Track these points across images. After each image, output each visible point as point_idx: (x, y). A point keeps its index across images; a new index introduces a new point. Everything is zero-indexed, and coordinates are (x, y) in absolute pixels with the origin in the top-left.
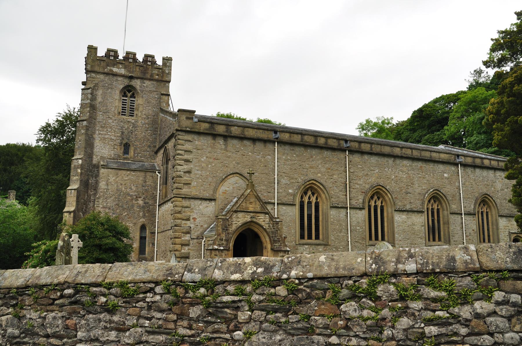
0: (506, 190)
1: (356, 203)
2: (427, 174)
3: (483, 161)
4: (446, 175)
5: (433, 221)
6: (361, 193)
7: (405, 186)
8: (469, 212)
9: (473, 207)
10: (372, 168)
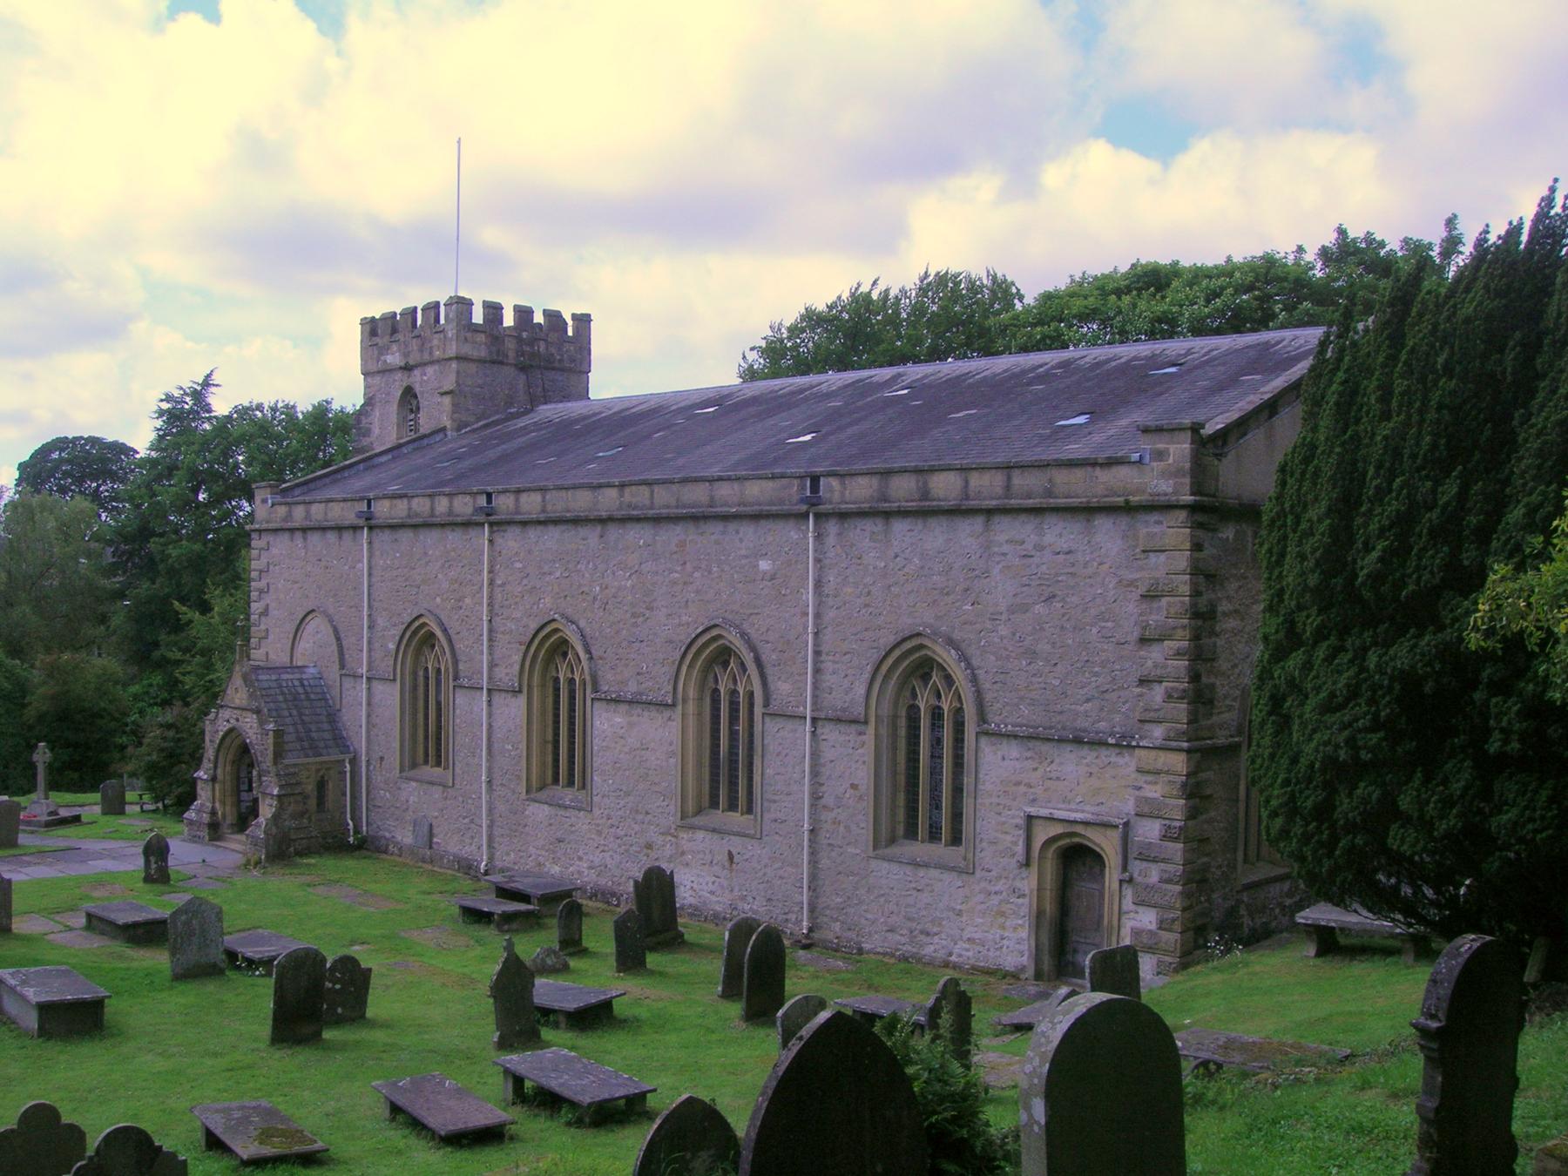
0: (1039, 608)
1: (507, 674)
2: (697, 568)
3: (925, 483)
4: (764, 565)
5: (733, 735)
6: (518, 645)
7: (628, 615)
8: (844, 710)
9: (861, 690)
10: (546, 569)
